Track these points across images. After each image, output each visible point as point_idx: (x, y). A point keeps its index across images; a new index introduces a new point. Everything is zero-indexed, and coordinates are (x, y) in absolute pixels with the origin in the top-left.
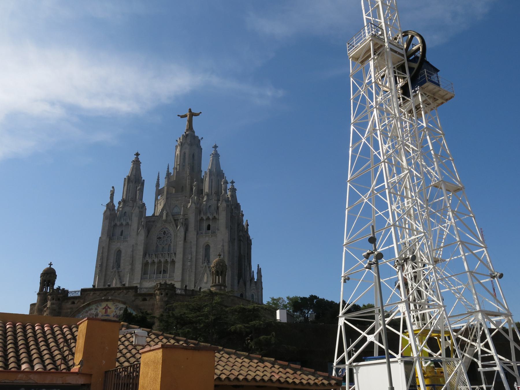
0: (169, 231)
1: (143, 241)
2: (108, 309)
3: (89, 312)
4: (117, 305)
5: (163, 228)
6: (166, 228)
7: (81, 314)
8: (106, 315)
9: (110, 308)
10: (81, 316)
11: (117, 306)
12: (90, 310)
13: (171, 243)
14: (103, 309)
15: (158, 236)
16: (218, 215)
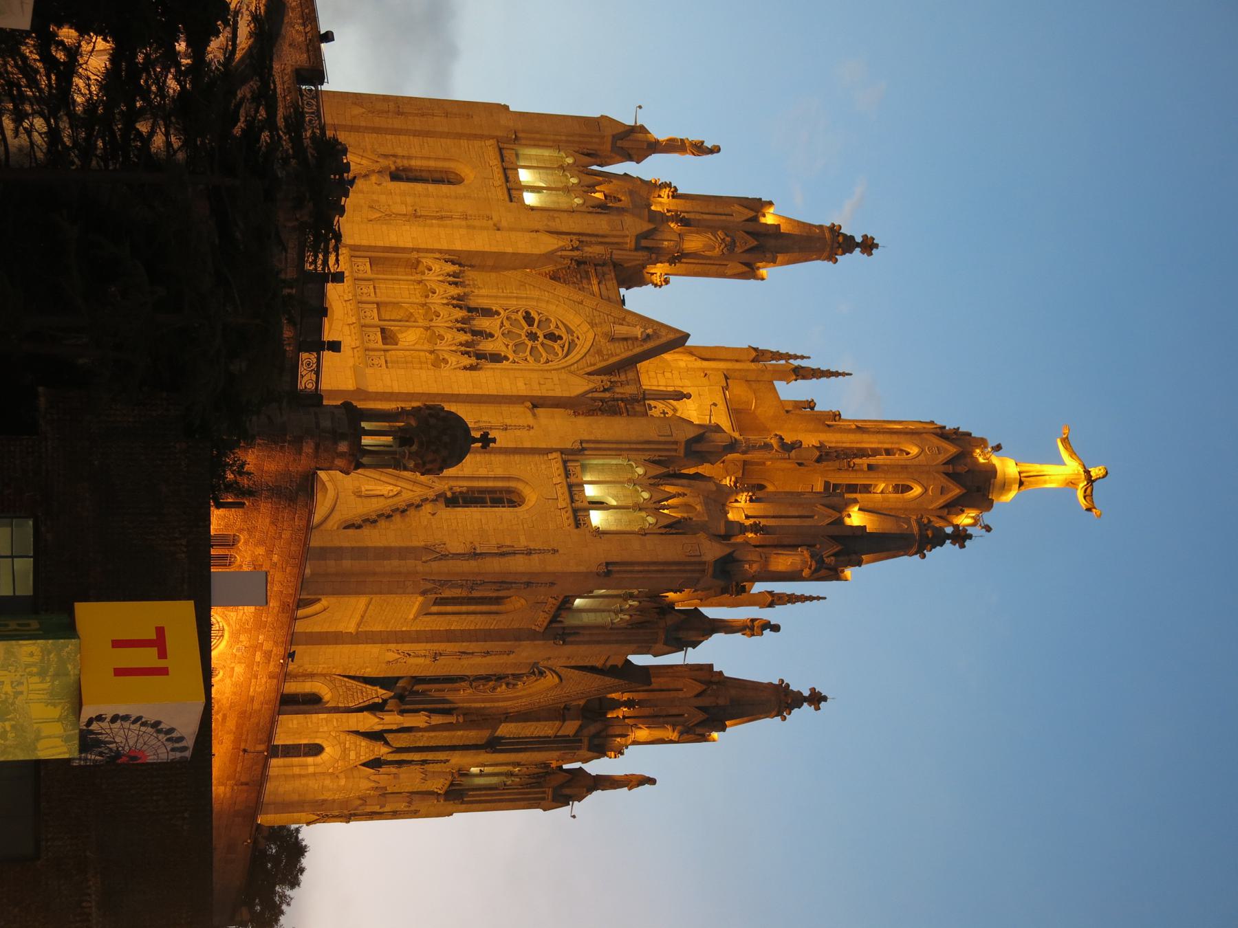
1: (510, 250)
5: (569, 331)
13: (514, 362)
16: (663, 531)
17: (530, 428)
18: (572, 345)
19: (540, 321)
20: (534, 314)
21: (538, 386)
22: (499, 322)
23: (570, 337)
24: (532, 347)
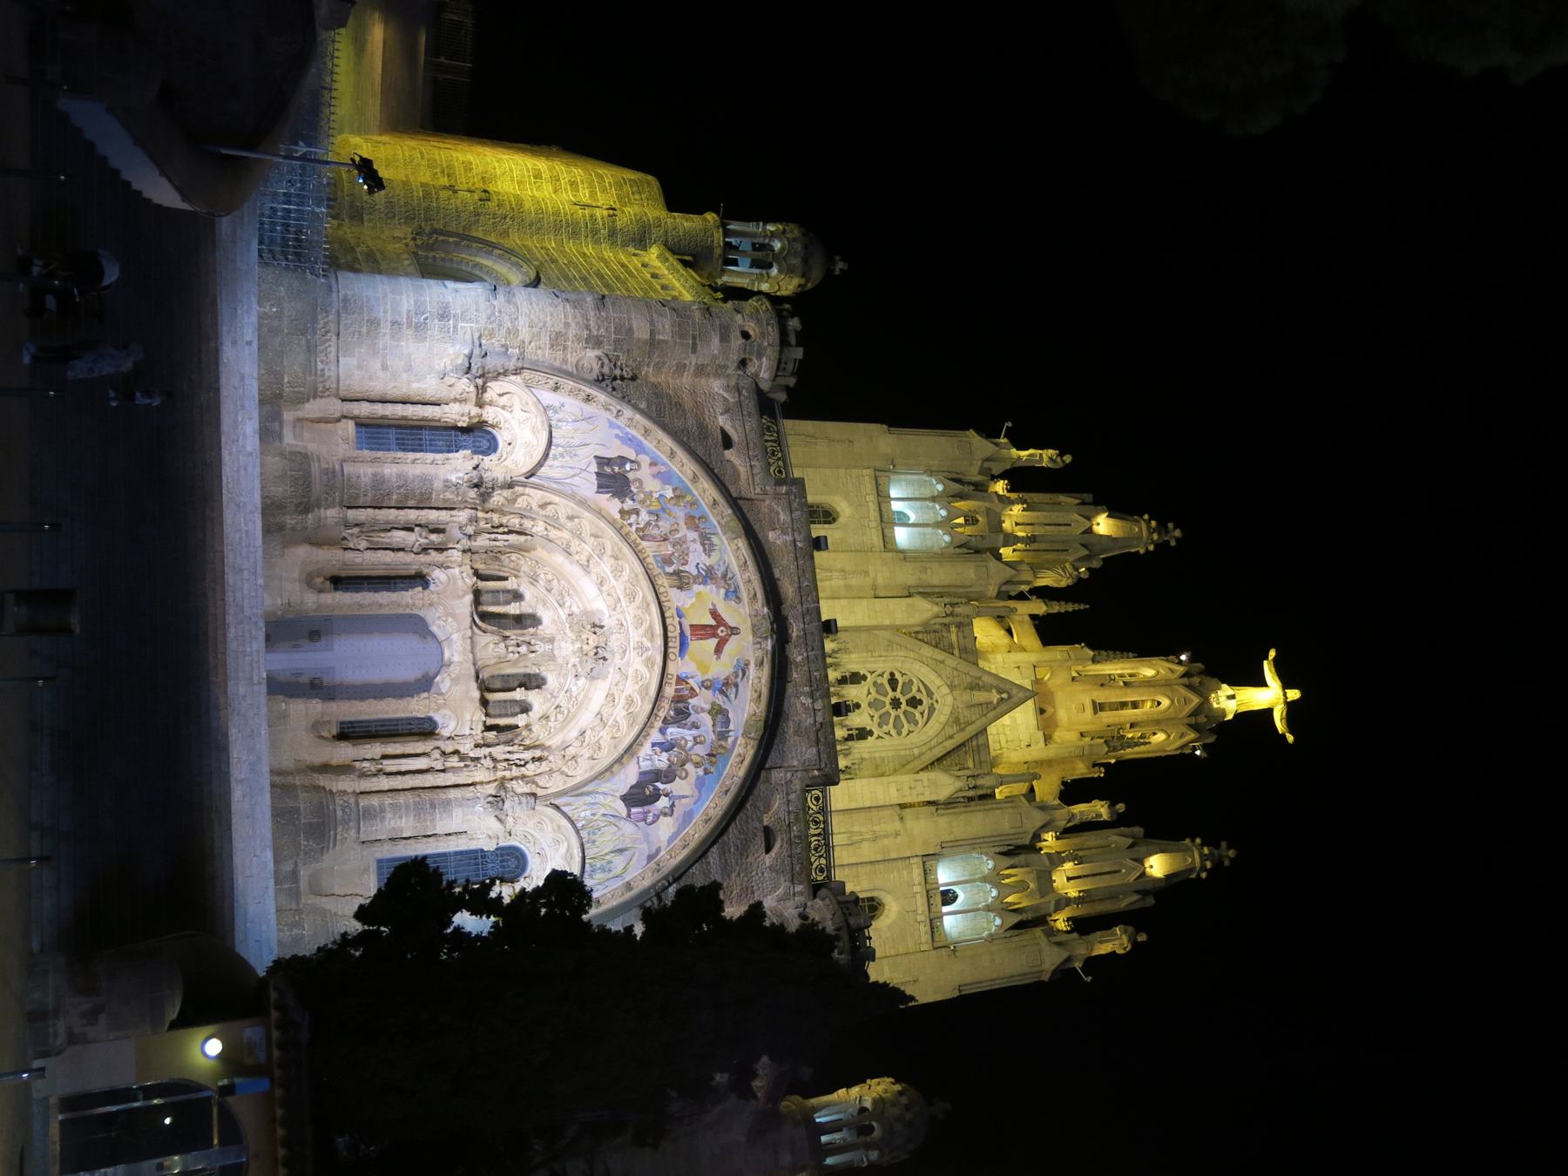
2: (713, 642)
3: (692, 535)
4: (736, 686)
5: (930, 694)
8: (682, 633)
9: (719, 650)
11: (734, 690)
12: (705, 539)
13: (879, 737)
14: (714, 614)
15: (903, 674)
17: (897, 835)
18: (932, 709)
19: (904, 683)
20: (898, 676)
21: (909, 791)
22: (866, 689)
23: (930, 701)
24: (896, 717)
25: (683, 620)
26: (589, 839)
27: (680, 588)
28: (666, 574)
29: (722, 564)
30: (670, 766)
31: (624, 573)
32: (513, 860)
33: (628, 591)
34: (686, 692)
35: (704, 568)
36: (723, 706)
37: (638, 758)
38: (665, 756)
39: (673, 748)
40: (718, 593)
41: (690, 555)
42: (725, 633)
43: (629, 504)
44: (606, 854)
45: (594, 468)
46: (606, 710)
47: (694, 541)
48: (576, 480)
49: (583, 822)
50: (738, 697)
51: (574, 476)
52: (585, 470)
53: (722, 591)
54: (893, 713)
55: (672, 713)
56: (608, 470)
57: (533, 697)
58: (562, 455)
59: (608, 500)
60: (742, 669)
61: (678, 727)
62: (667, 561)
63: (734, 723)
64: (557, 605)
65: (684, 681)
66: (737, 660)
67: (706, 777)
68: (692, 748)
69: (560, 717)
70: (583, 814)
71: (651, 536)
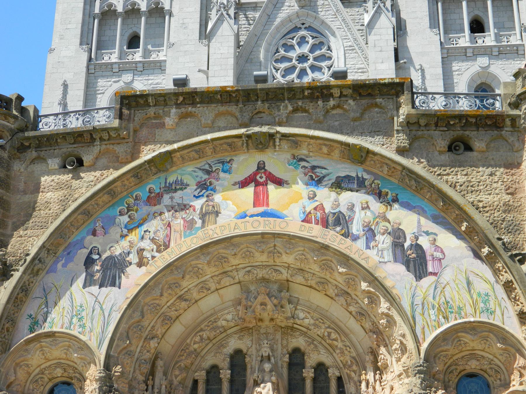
0: (323, 39)
4: (314, 168)
6: (305, 28)
7: (124, 208)
8: (264, 214)
9: (279, 182)
10: (125, 219)
11: (318, 170)
21: (383, 53)
25: (248, 213)
26: (456, 313)
27: (217, 213)
28: (203, 226)
29: (196, 174)
30: (389, 233)
31: (200, 266)
32: (470, 387)
33: (217, 263)
34: (319, 214)
35: (198, 190)
36: (333, 181)
37: (380, 262)
38: (379, 237)
39: (372, 229)
40: (224, 179)
41: (185, 203)
42: (263, 175)
43: (133, 258)
44: (472, 297)
45: (94, 289)
46: (331, 291)
47: (172, 198)
48: (107, 307)
49: (441, 317)
50: (326, 167)
51: (101, 308)
52: (96, 298)
53: (222, 175)
54: (311, 62)
55: (338, 229)
56: (98, 276)
57: (312, 360)
58: (80, 319)
59: (127, 277)
60: (299, 161)
61: (352, 224)
62: (190, 225)
63: (350, 172)
64: (224, 335)
65: (307, 215)
66: (290, 165)
67: (400, 201)
68: (372, 212)
69: (333, 336)
70: (433, 317)
71: (164, 238)
